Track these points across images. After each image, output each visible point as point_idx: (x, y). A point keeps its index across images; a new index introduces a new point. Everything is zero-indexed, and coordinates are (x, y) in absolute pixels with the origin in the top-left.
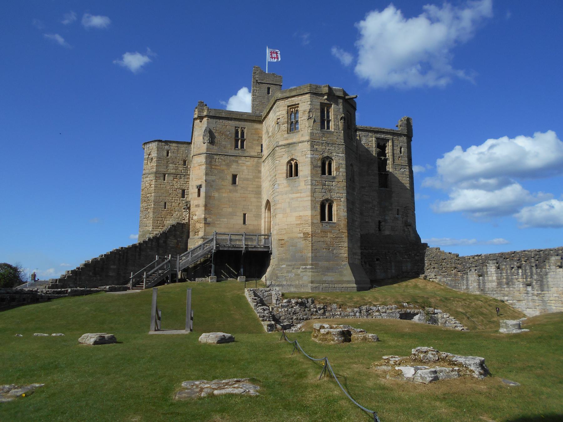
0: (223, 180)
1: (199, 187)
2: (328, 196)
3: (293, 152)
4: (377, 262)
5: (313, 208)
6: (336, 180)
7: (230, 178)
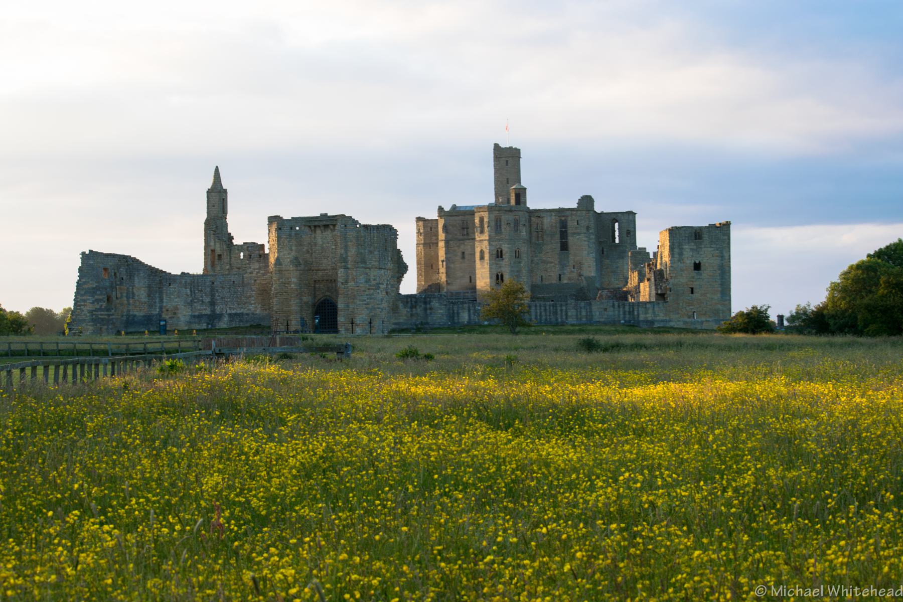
5: (491, 278)
7: (460, 254)
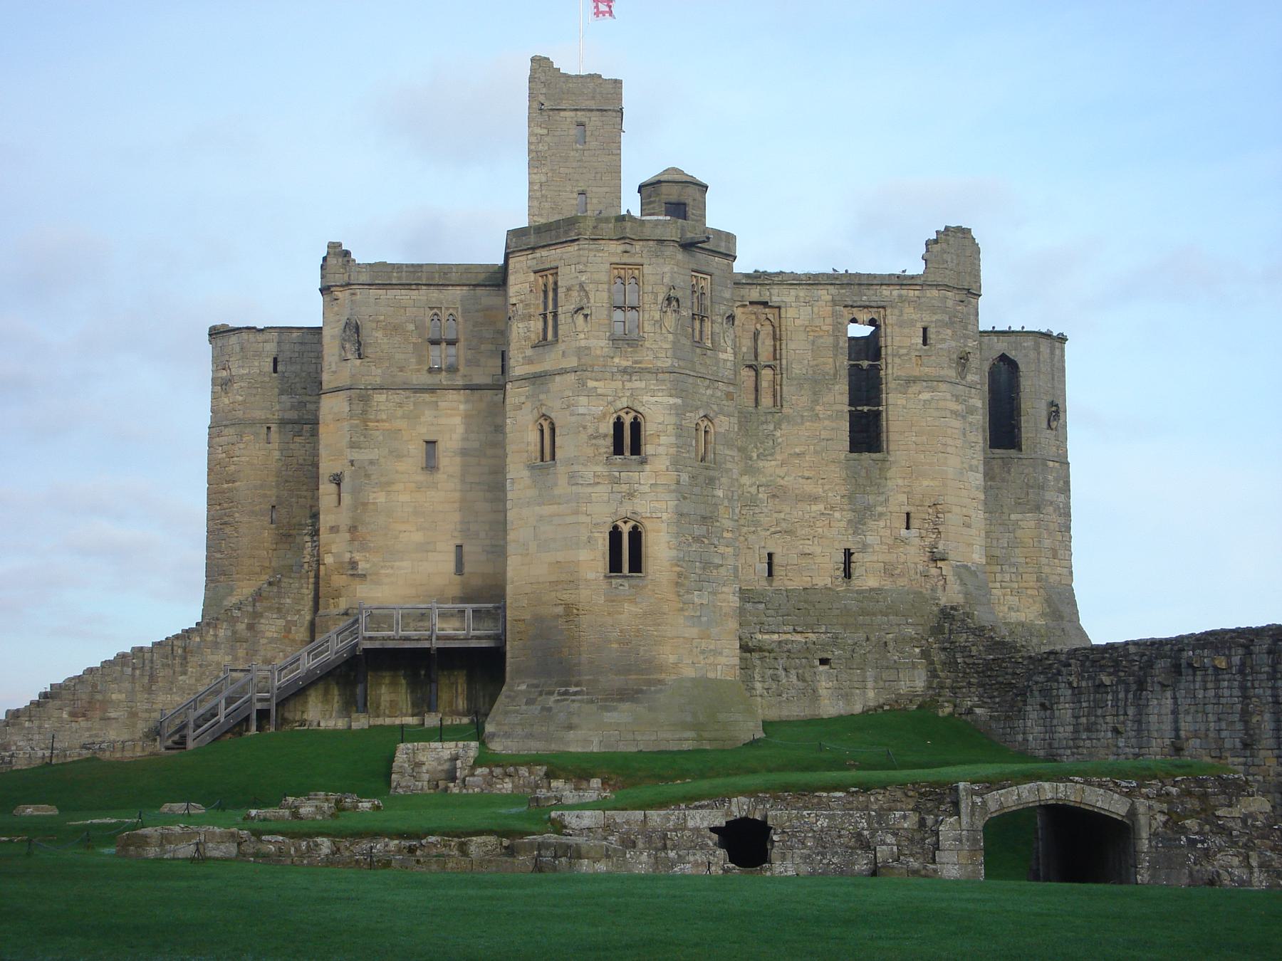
0: (399, 456)
1: (337, 480)
2: (626, 509)
3: (542, 397)
4: (822, 668)
6: (648, 467)
7: (416, 450)
